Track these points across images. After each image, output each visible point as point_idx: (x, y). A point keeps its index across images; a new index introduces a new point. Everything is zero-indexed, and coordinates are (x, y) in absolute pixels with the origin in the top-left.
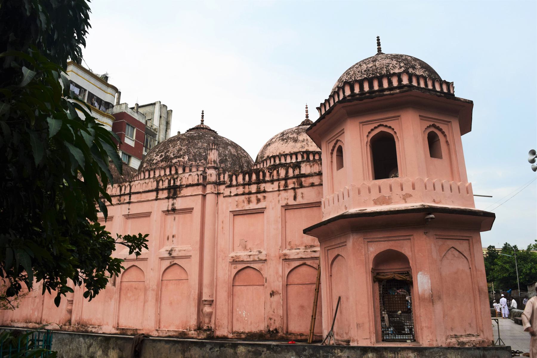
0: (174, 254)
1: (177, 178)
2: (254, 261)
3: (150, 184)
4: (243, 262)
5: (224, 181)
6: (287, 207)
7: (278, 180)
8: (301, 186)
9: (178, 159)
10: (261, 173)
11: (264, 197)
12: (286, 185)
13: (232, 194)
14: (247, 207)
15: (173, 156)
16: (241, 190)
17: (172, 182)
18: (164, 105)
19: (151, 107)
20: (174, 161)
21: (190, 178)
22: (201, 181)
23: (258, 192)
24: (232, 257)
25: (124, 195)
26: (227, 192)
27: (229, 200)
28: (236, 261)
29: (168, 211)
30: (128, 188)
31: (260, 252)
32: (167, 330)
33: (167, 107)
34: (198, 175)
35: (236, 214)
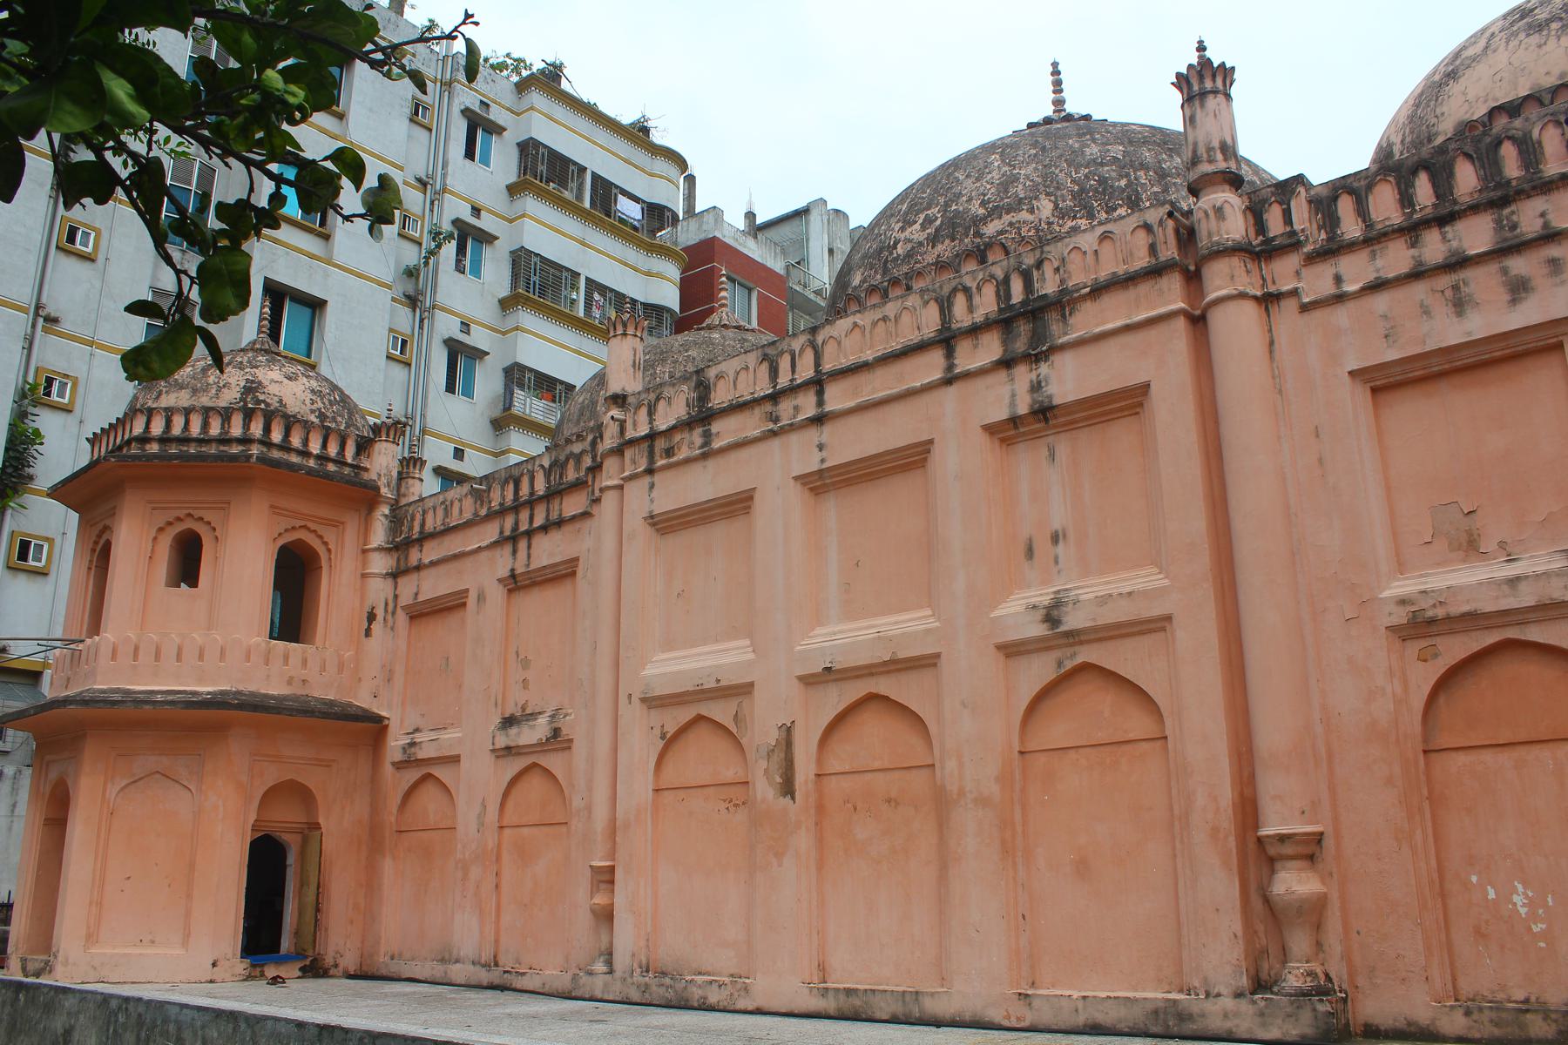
0: (1074, 620)
1: (1039, 265)
3: (906, 318)
4: (1472, 620)
5: (1293, 233)
9: (1007, 218)
14: (1450, 331)
15: (981, 211)
16: (1396, 258)
17: (1017, 287)
18: (837, 211)
19: (796, 222)
20: (991, 229)
21: (1107, 248)
22: (1169, 251)
24: (1403, 602)
25: (793, 389)
26: (1318, 282)
27: (1341, 316)
28: (1432, 621)
29: (1014, 421)
30: (809, 356)
32: (1076, 994)
33: (846, 216)
34: (1147, 227)
35: (1383, 383)
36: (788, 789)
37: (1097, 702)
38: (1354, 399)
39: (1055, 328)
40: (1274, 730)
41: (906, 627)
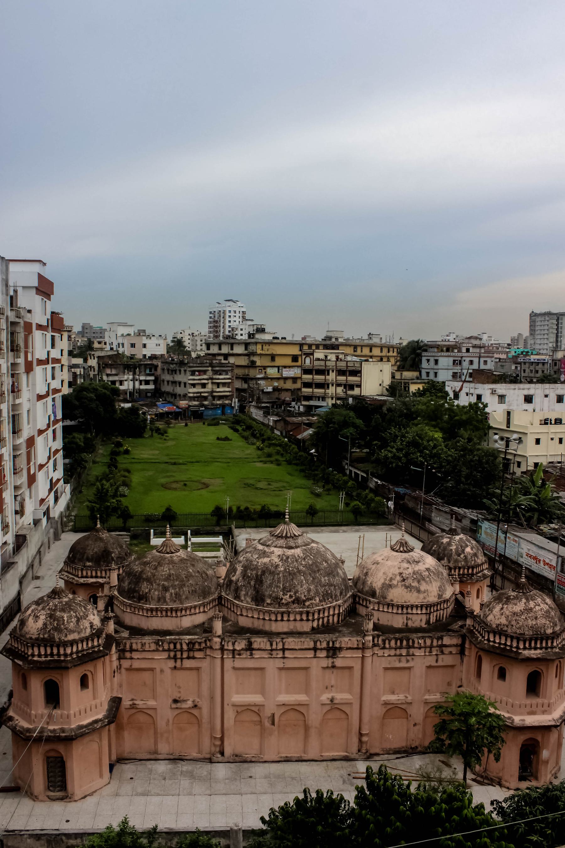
0: (335, 702)
2: (402, 704)
3: (306, 643)
4: (393, 704)
6: (430, 667)
7: (425, 647)
8: (442, 653)
9: (310, 602)
10: (411, 641)
11: (413, 659)
12: (430, 652)
13: (386, 655)
16: (393, 652)
22: (361, 646)
23: (408, 655)
26: (380, 653)
27: (383, 658)
29: (327, 667)
31: (406, 697)
35: (386, 669)
36: (273, 724)
37: (338, 714)
38: (382, 670)
39: (338, 653)
40: (366, 719)
41: (302, 698)
